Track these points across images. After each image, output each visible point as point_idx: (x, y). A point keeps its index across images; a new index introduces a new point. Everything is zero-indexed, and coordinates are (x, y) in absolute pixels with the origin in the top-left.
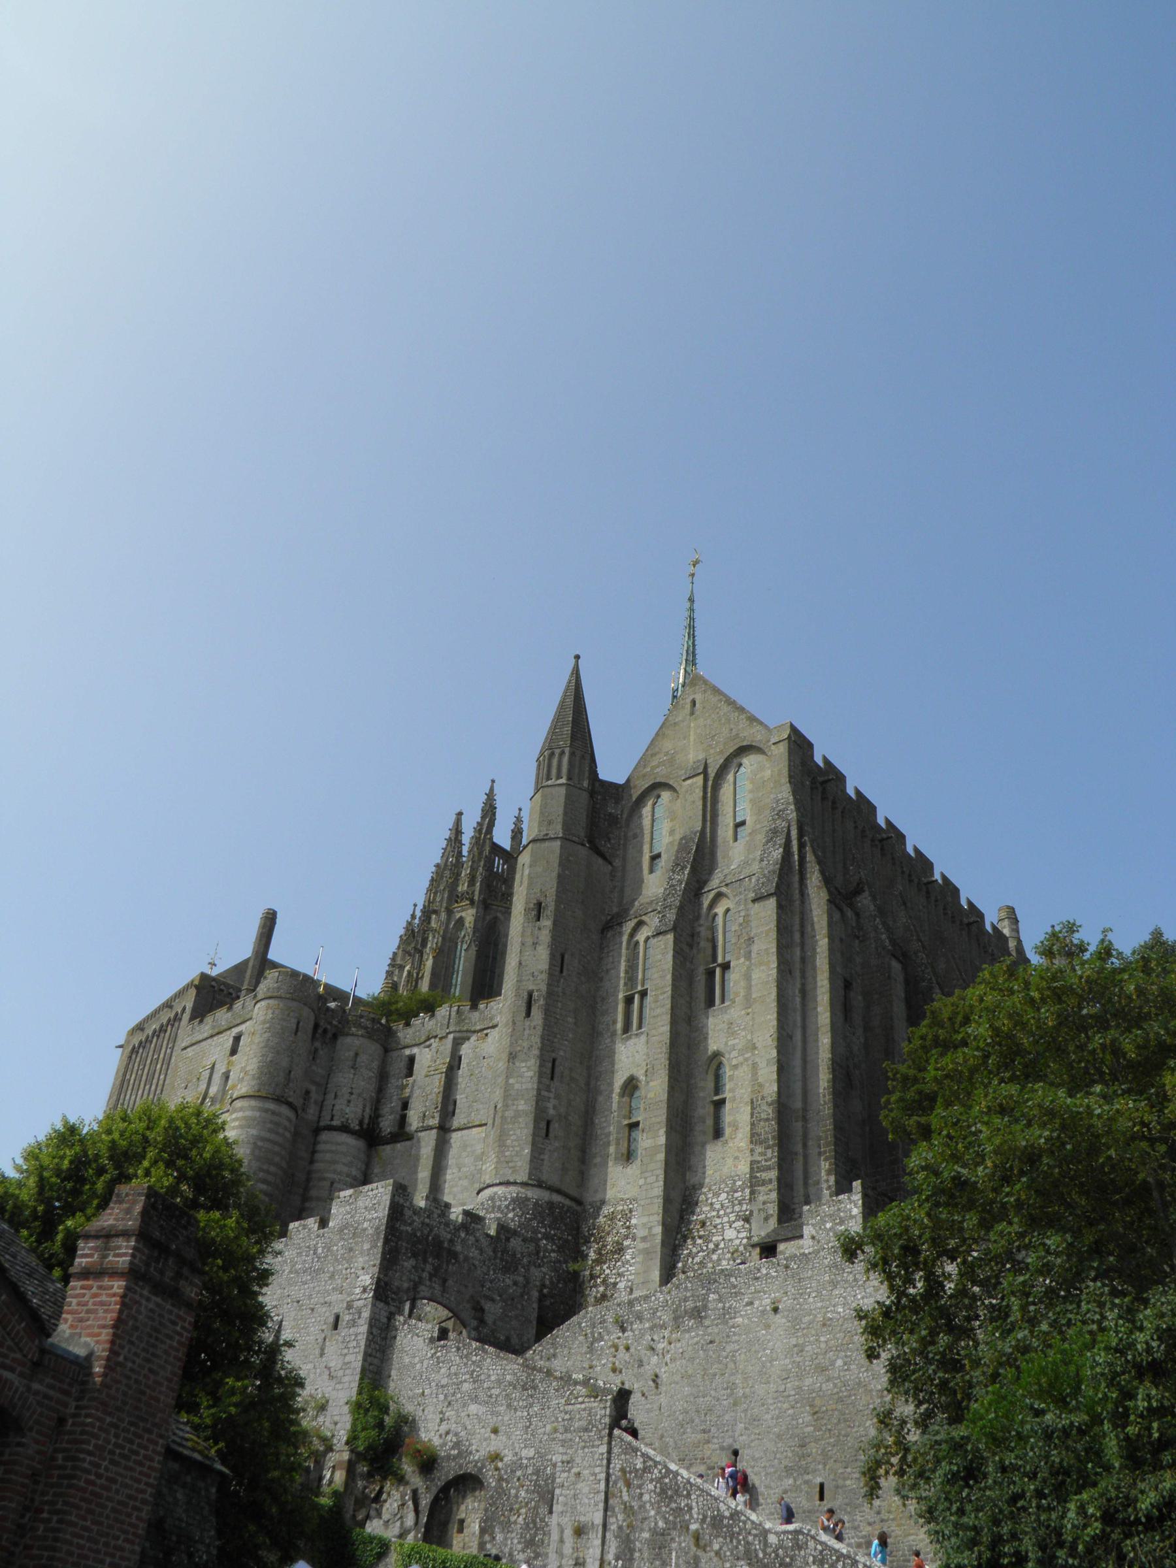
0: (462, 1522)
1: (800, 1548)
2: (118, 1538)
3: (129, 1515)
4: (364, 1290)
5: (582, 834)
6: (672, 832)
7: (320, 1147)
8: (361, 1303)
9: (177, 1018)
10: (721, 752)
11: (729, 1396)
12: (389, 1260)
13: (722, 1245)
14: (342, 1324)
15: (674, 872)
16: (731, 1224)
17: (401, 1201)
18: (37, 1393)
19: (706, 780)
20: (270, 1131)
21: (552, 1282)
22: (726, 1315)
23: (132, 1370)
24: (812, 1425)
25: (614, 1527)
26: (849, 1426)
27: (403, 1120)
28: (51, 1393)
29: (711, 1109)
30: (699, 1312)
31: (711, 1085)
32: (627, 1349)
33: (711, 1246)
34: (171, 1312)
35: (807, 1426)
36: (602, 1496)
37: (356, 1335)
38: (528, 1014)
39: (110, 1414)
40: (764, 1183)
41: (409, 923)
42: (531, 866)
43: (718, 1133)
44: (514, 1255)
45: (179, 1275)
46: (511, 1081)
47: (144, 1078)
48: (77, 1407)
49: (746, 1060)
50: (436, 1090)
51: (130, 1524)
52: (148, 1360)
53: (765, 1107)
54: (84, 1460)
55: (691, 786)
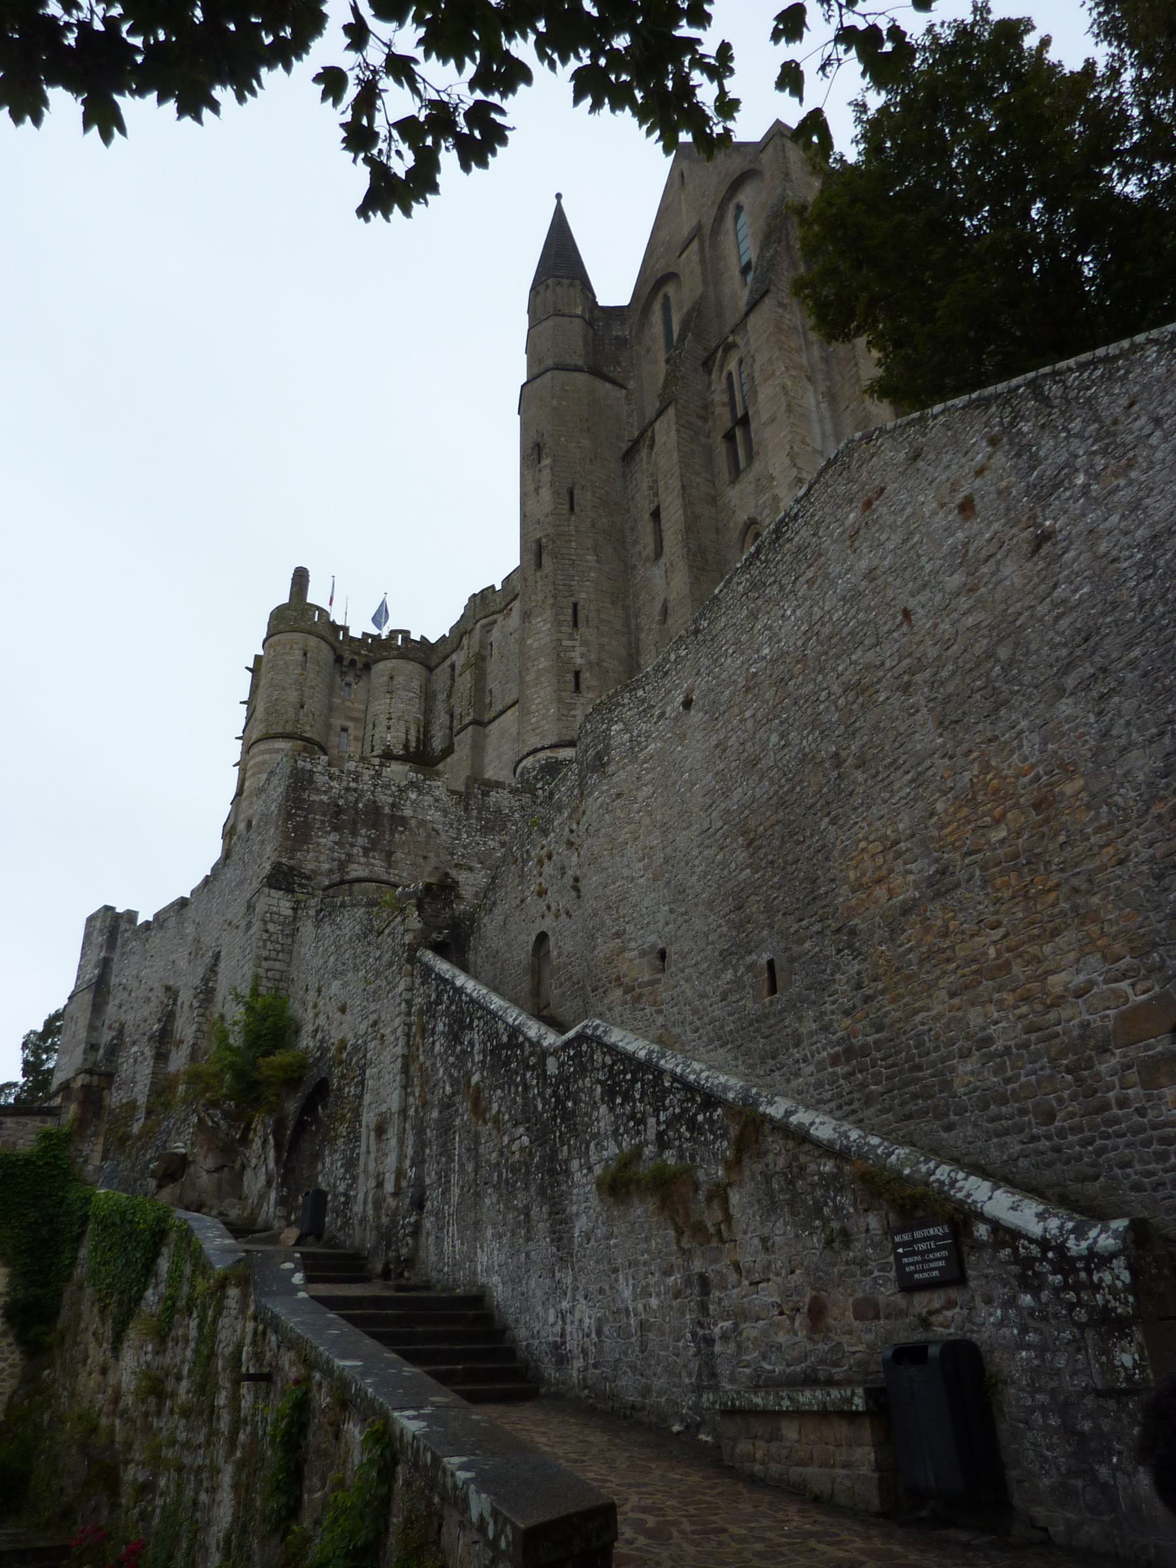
10: (714, 202)
11: (646, 868)
17: (308, 766)
19: (702, 244)
24: (748, 866)
26: (798, 843)
27: (451, 728)
30: (601, 759)
35: (742, 870)
38: (539, 565)
44: (499, 811)
46: (529, 642)
50: (469, 685)
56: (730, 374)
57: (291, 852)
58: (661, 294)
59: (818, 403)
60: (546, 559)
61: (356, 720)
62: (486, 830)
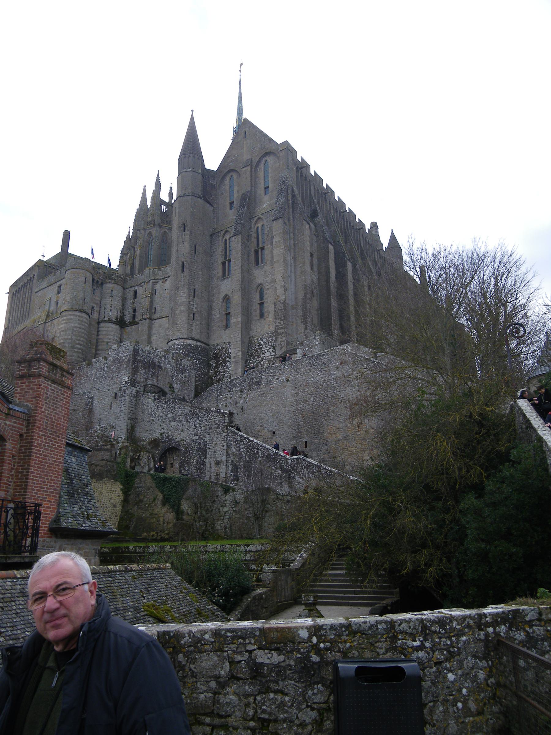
0: (172, 464)
1: (300, 464)
2: (51, 476)
3: (55, 468)
4: (126, 383)
5: (200, 194)
6: (238, 192)
7: (100, 329)
8: (125, 388)
9: (31, 280)
10: (258, 155)
11: (270, 413)
12: (135, 371)
13: (265, 358)
14: (118, 396)
15: (239, 209)
16: (268, 350)
18: (9, 425)
19: (251, 168)
20: (79, 324)
21: (199, 376)
22: (269, 383)
23: (48, 414)
25: (230, 461)
27: (134, 316)
28: (15, 425)
29: (258, 306)
31: (258, 296)
32: (231, 398)
33: (260, 359)
34: (61, 390)
36: (225, 451)
37: (124, 400)
38: (183, 271)
39: (41, 431)
40: (280, 334)
41: (128, 236)
42: (179, 208)
43: (262, 315)
44: (184, 366)
45: (62, 375)
46: (177, 299)
47: (20, 306)
48: (27, 430)
49: (272, 286)
51: (56, 471)
52: (54, 410)
53: (280, 305)
54: (34, 449)
55: (245, 171)
56: (258, 227)
57: (134, 375)
58: (230, 174)
59: (291, 260)
60: (185, 270)
61: (97, 304)
62: (182, 372)
